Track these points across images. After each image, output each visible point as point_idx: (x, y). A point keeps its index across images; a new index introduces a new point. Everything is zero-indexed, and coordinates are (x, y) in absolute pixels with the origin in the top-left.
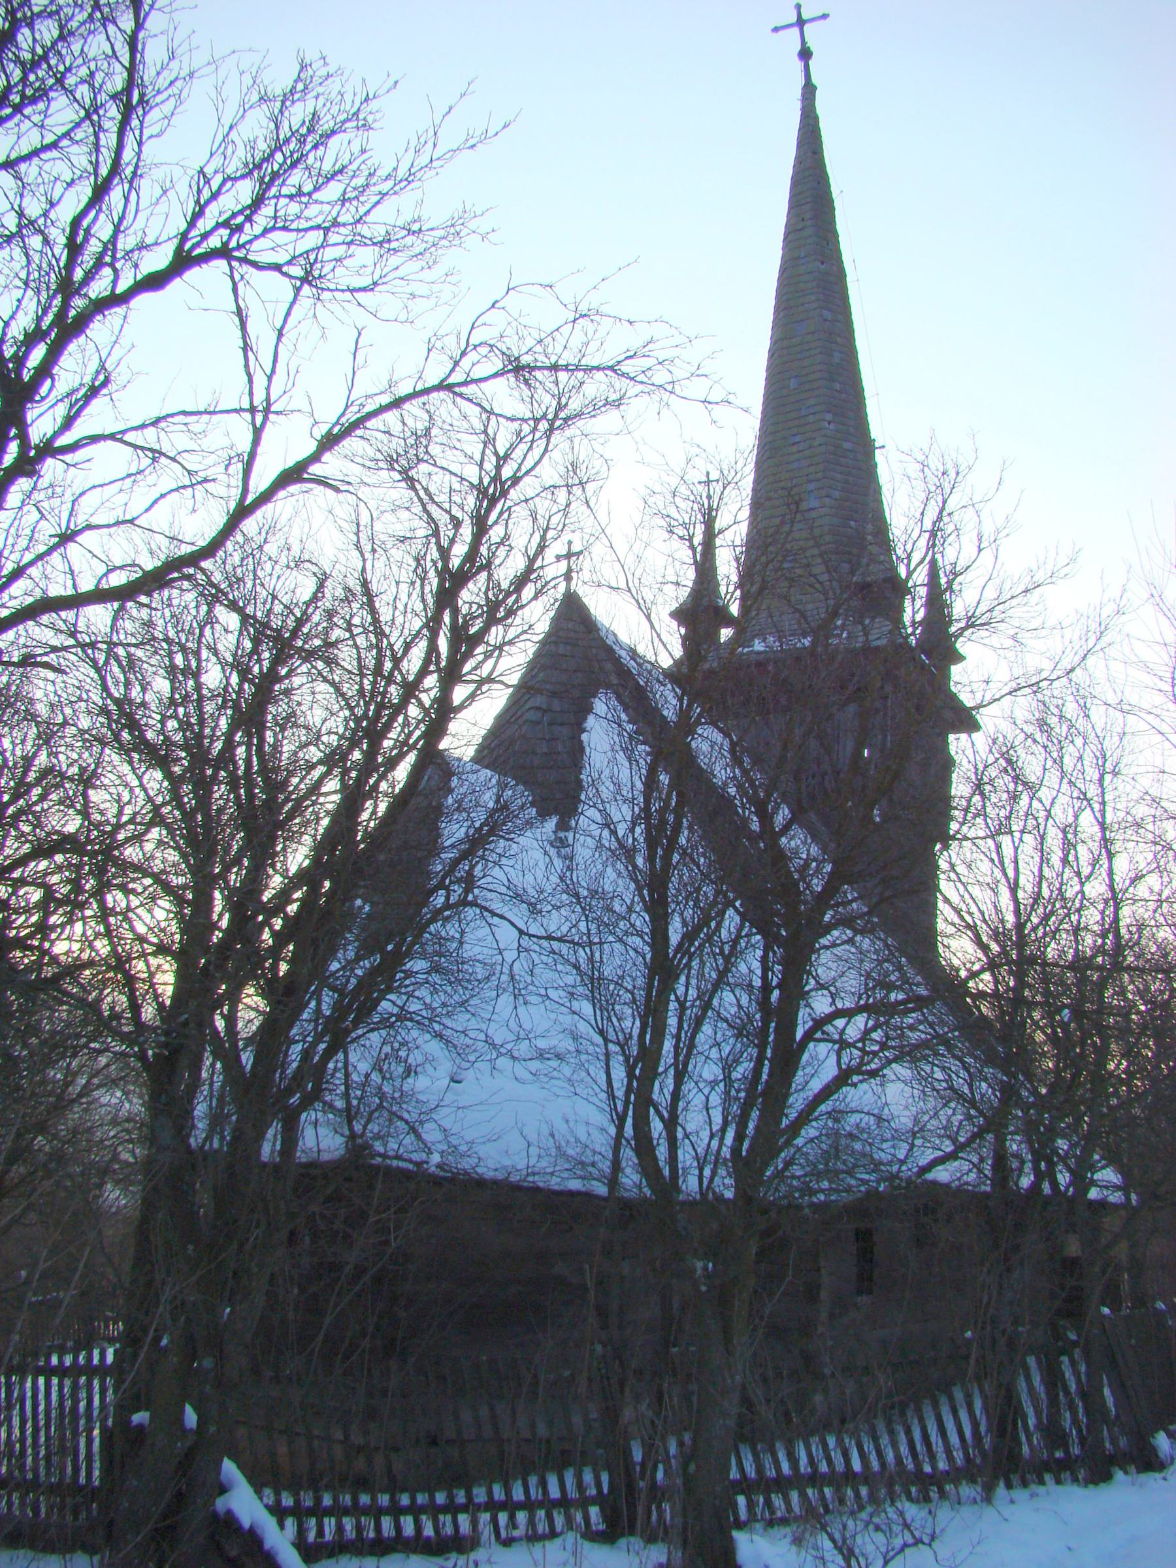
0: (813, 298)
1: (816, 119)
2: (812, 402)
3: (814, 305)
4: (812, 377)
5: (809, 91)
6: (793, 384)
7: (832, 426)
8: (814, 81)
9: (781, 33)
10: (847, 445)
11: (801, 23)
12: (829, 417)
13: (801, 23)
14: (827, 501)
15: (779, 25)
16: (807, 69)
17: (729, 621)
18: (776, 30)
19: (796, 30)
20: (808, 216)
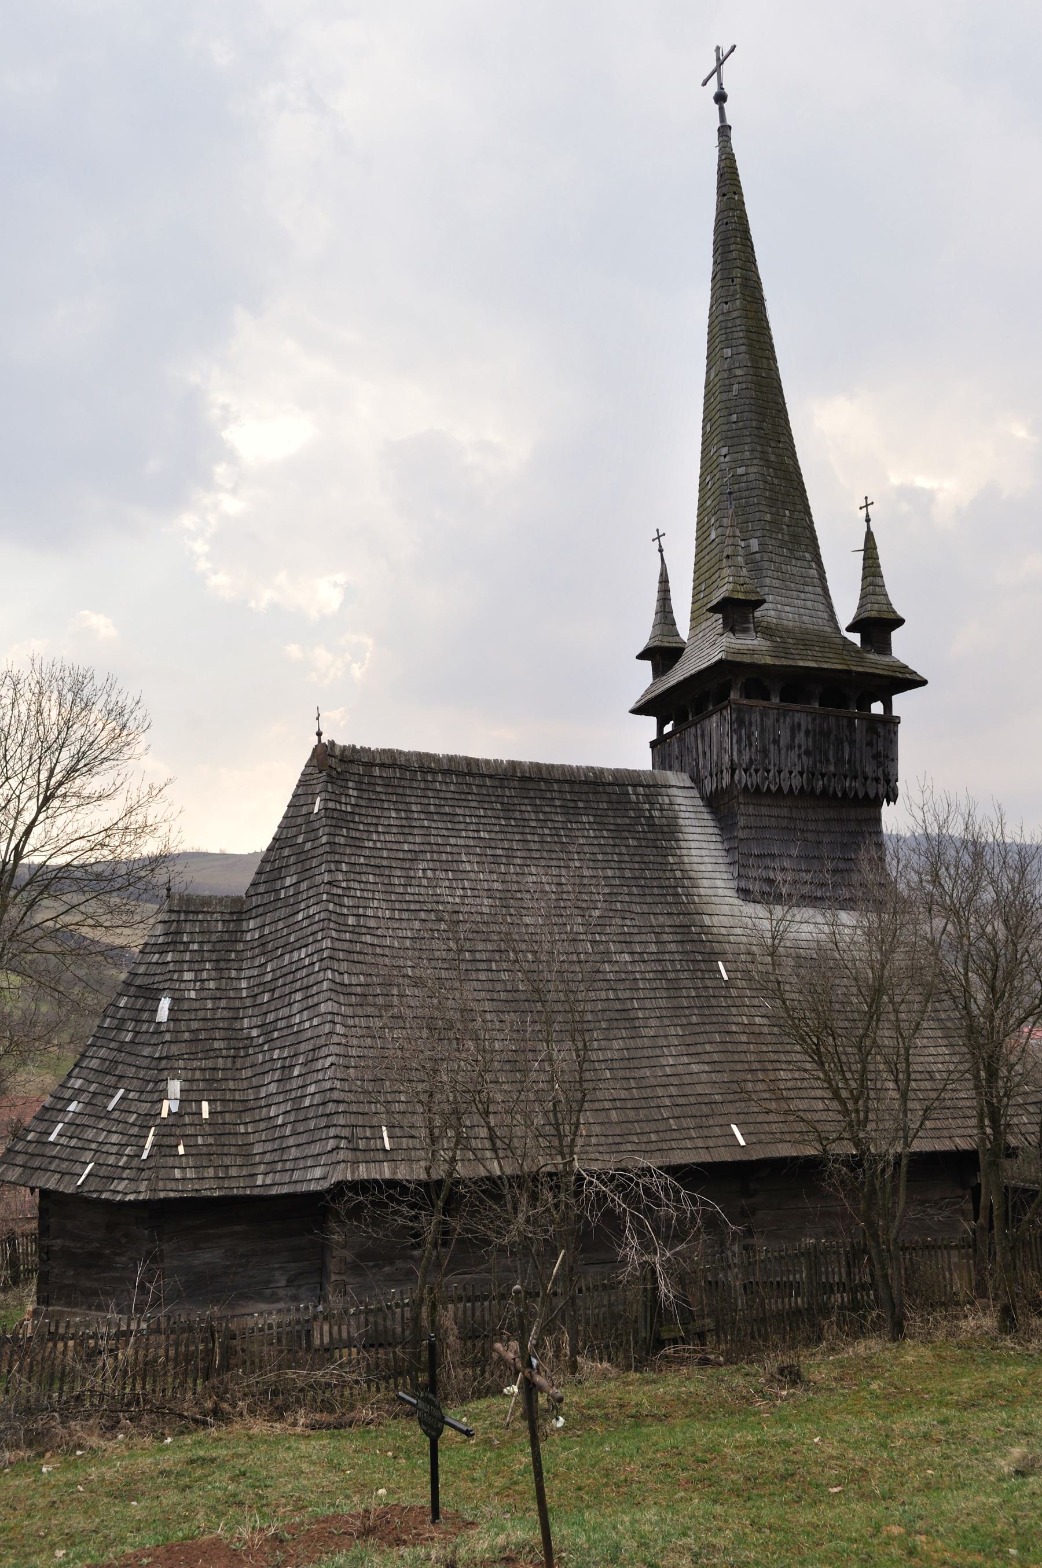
5: (724, 131)
7: (728, 458)
10: (741, 471)
15: (705, 77)
16: (722, 110)
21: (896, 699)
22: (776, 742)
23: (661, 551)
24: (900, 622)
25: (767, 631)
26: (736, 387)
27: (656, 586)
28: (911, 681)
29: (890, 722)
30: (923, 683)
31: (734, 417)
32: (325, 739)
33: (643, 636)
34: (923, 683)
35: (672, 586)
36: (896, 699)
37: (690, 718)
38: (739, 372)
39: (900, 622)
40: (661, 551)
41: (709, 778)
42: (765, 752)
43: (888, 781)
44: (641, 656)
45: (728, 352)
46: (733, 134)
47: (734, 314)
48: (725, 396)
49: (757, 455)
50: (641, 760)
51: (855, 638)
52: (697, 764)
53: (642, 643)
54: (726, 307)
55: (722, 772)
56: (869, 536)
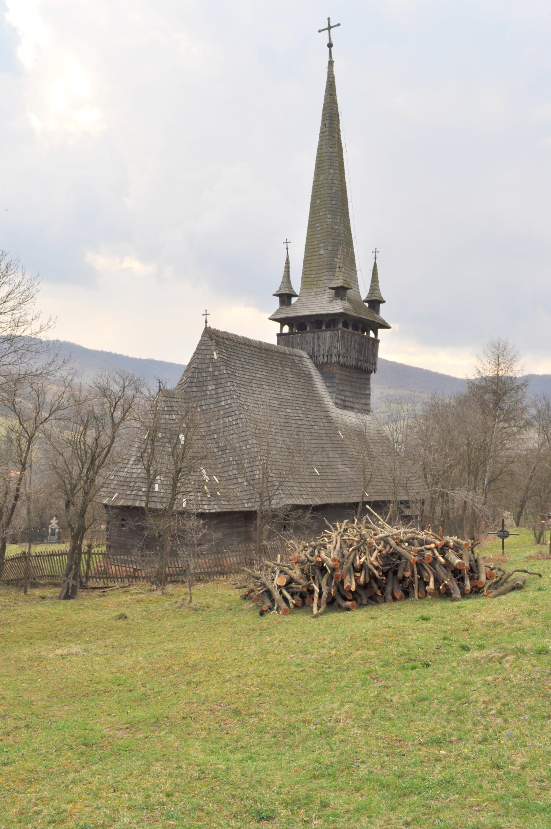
0: (326, 164)
1: (333, 77)
2: (324, 210)
3: (326, 168)
4: (324, 199)
5: (331, 63)
6: (318, 201)
7: (330, 220)
8: (334, 59)
9: (327, 21)
10: (336, 227)
11: (329, 28)
12: (329, 216)
13: (329, 28)
14: (327, 251)
15: (321, 29)
17: (296, 296)
18: (320, 31)
19: (327, 31)
20: (327, 125)
21: (380, 331)
22: (350, 346)
23: (287, 249)
24: (384, 302)
25: (349, 301)
26: (334, 188)
27: (283, 264)
28: (385, 326)
29: (376, 342)
30: (389, 327)
31: (334, 202)
32: (208, 326)
33: (276, 285)
34: (389, 327)
35: (291, 265)
36: (380, 331)
37: (308, 329)
38: (336, 182)
39: (384, 302)
40: (287, 249)
41: (322, 356)
42: (347, 349)
43: (375, 365)
44: (274, 295)
45: (332, 171)
46: (335, 64)
47: (335, 154)
48: (330, 191)
49: (342, 221)
50: (273, 340)
51: (367, 305)
52: (313, 350)
53: (275, 289)
54: (331, 149)
55: (331, 356)
56: (375, 265)
